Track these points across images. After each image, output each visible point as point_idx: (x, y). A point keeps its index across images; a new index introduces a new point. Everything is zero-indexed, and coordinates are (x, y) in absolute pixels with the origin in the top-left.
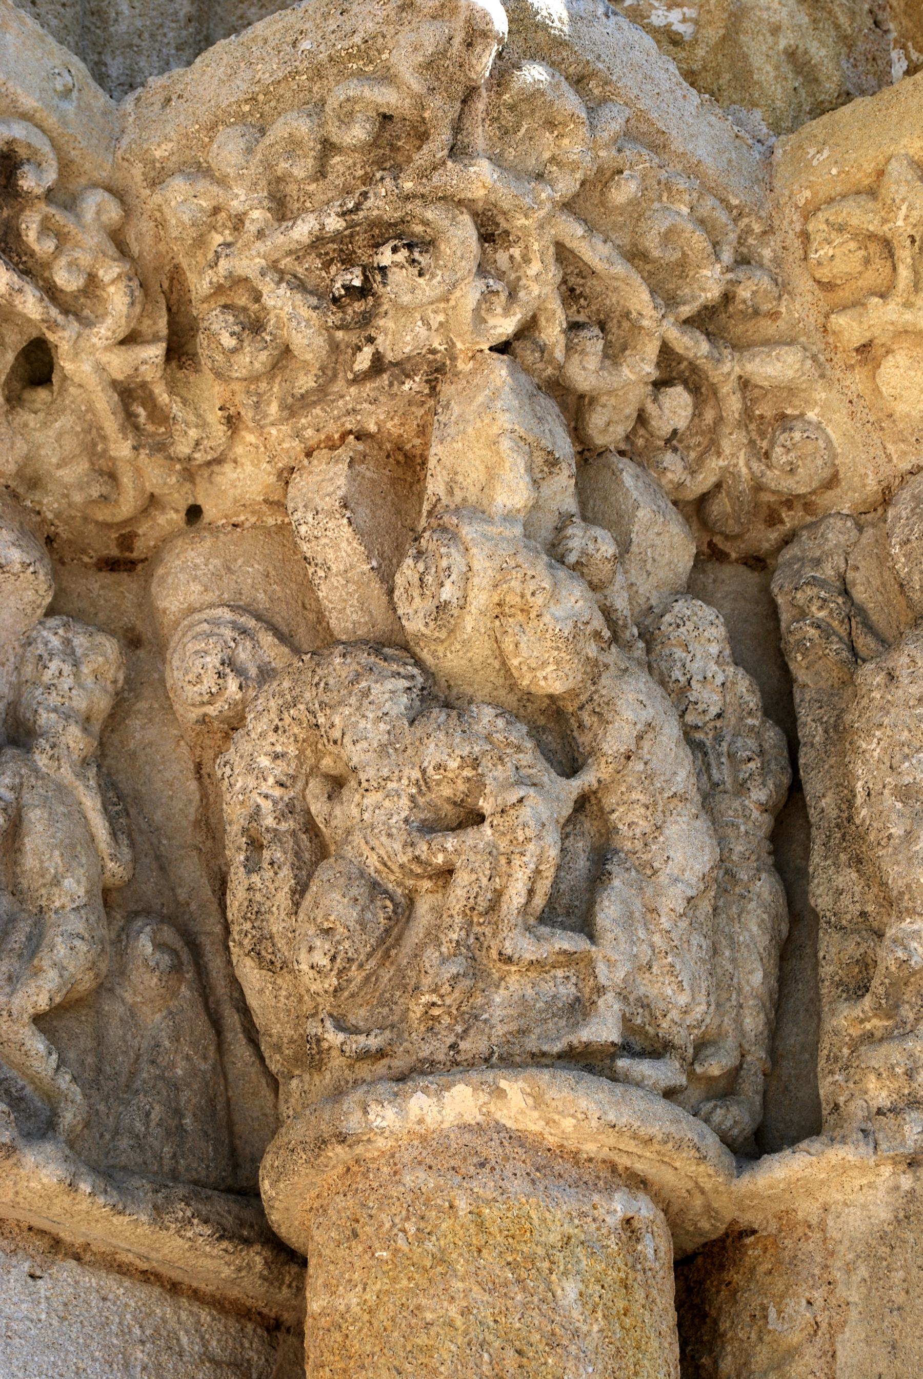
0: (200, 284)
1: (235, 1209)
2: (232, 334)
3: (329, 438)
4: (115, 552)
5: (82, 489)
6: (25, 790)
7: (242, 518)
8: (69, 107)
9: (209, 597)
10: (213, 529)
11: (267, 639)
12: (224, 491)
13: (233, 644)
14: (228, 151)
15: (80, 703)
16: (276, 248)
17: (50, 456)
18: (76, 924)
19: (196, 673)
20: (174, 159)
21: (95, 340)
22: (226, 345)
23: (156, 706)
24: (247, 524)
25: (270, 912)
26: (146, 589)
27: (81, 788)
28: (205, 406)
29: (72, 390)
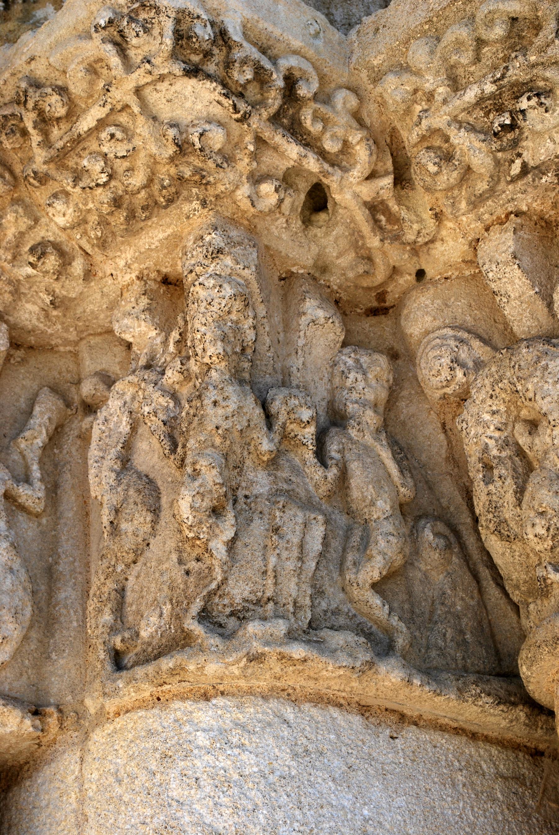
0: (410, 136)
1: (504, 685)
2: (435, 164)
3: (498, 218)
4: (375, 304)
5: (353, 269)
6: (346, 452)
7: (450, 273)
8: (319, 43)
9: (437, 323)
10: (434, 282)
11: (476, 343)
12: (438, 259)
13: (456, 349)
14: (419, 54)
15: (370, 396)
16: (455, 108)
17: (332, 252)
18: (388, 527)
19: (436, 370)
20: (385, 64)
21: (351, 179)
22: (431, 171)
23: (413, 392)
24: (453, 277)
25: (503, 506)
26: (397, 324)
27: (378, 446)
28: (420, 209)
29: (340, 211)
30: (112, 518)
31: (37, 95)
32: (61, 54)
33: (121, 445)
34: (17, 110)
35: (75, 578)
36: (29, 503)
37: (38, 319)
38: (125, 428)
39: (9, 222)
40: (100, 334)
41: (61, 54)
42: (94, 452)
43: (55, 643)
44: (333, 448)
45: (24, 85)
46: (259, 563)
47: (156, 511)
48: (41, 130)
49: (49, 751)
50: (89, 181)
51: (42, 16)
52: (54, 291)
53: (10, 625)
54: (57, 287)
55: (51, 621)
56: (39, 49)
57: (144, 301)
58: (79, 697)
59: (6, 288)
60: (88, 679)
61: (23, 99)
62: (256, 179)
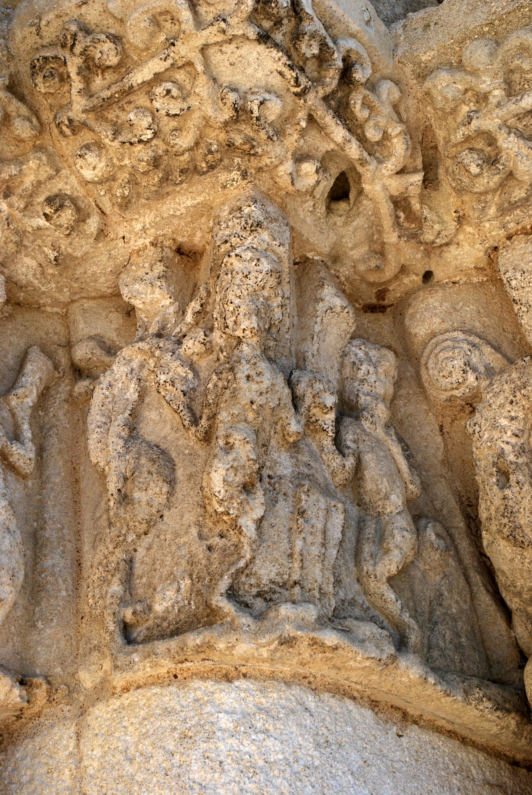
1: (501, 692)
2: (478, 165)
3: (524, 228)
4: (374, 301)
5: (365, 262)
6: (360, 443)
7: (458, 278)
9: (445, 326)
11: (487, 350)
12: (450, 262)
13: (469, 353)
14: (478, 54)
16: (509, 112)
19: (450, 371)
20: (434, 61)
21: (384, 171)
22: (473, 172)
23: (411, 392)
24: (461, 282)
25: (519, 512)
27: (389, 441)
28: (442, 211)
29: (365, 202)
30: (120, 486)
31: (88, 40)
33: (129, 412)
34: (62, 53)
36: (20, 463)
37: (34, 275)
38: (132, 394)
39: (30, 168)
40: (94, 298)
42: (95, 416)
43: (41, 611)
44: (349, 438)
45: (74, 28)
46: (284, 545)
47: (172, 482)
48: (84, 77)
49: (30, 725)
50: (130, 136)
52: (60, 247)
54: (64, 244)
55: (36, 589)
57: (159, 268)
58: (70, 670)
59: (13, 238)
60: (81, 651)
61: (70, 42)
62: (300, 158)
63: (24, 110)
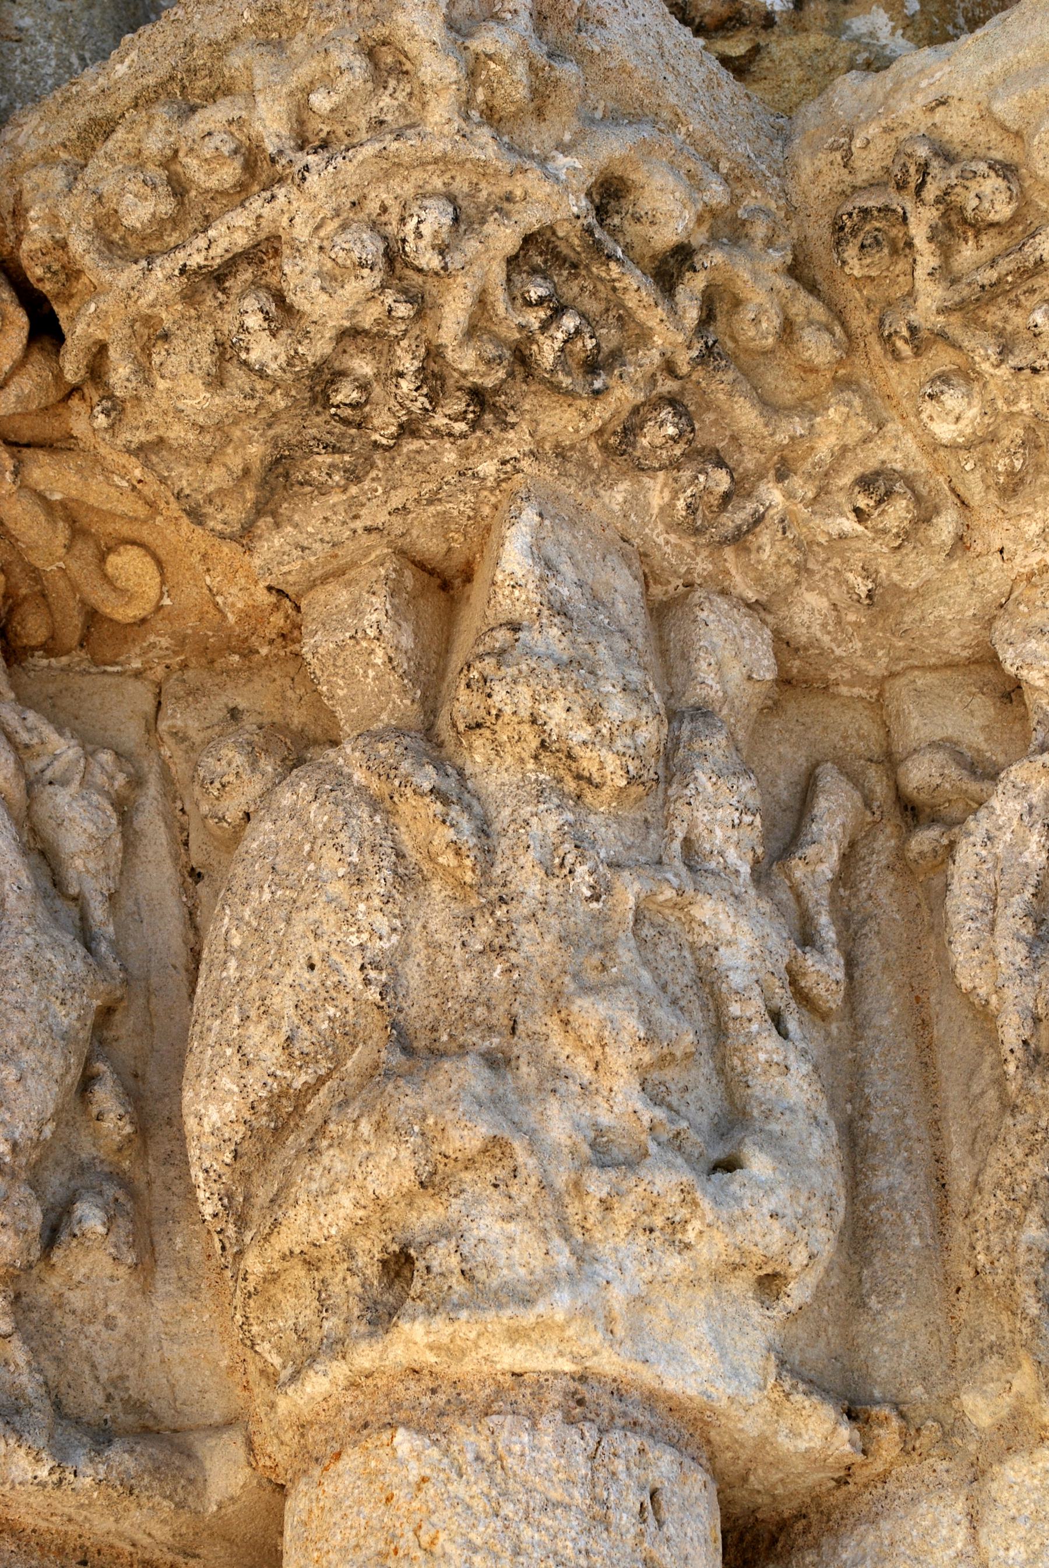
30: (1026, 1034)
31: (953, 174)
32: (1023, 97)
33: (1032, 890)
34: (903, 202)
35: (908, 1150)
36: (820, 990)
37: (824, 626)
39: (829, 423)
40: (934, 668)
41: (1023, 97)
42: (963, 899)
43: (873, 1276)
45: (923, 152)
48: (941, 245)
49: (867, 1497)
50: (1031, 356)
51: (864, 30)
52: (877, 572)
53: (821, 1231)
54: (884, 567)
55: (860, 1232)
56: (961, 83)
58: (941, 1391)
59: (791, 556)
60: (961, 1354)
61: (914, 179)
63: (819, 312)
